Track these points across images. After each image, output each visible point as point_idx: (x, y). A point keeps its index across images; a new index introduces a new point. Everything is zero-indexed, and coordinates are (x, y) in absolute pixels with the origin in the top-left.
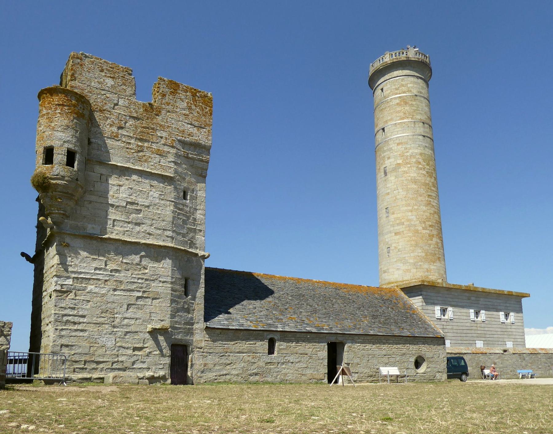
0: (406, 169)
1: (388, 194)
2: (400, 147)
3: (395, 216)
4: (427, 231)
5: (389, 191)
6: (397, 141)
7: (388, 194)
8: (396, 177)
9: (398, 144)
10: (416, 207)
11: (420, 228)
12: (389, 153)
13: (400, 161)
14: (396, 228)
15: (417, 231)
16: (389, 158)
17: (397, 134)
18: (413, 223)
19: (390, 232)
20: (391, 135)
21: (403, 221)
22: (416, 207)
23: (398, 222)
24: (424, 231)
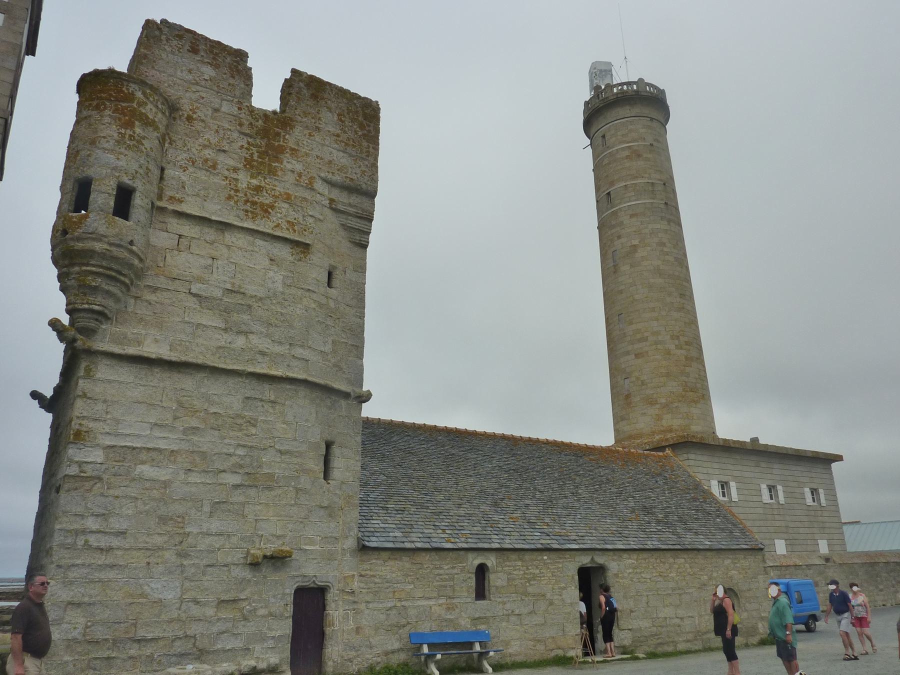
0: (645, 254)
1: (621, 292)
2: (634, 219)
3: (634, 327)
4: (682, 351)
5: (623, 287)
6: (630, 212)
7: (621, 292)
8: (632, 266)
9: (632, 216)
10: (664, 313)
11: (672, 347)
12: (618, 229)
13: (636, 242)
14: (636, 346)
15: (668, 352)
16: (619, 237)
17: (630, 201)
18: (660, 338)
19: (628, 353)
20: (620, 203)
21: (646, 334)
22: (664, 313)
23: (638, 336)
24: (679, 352)
